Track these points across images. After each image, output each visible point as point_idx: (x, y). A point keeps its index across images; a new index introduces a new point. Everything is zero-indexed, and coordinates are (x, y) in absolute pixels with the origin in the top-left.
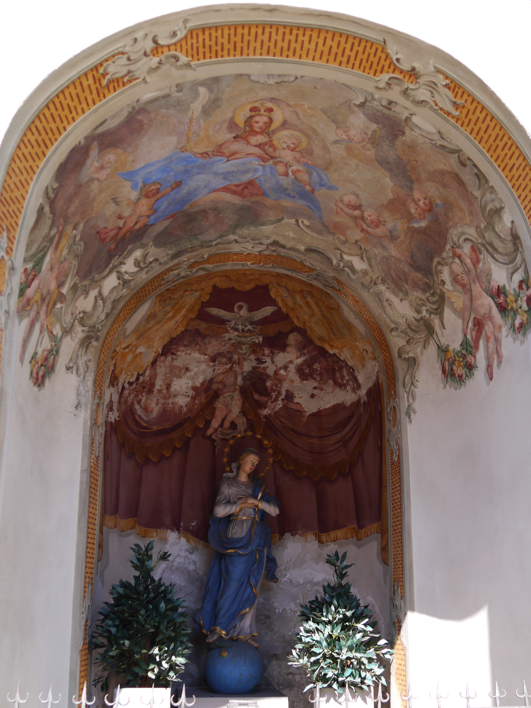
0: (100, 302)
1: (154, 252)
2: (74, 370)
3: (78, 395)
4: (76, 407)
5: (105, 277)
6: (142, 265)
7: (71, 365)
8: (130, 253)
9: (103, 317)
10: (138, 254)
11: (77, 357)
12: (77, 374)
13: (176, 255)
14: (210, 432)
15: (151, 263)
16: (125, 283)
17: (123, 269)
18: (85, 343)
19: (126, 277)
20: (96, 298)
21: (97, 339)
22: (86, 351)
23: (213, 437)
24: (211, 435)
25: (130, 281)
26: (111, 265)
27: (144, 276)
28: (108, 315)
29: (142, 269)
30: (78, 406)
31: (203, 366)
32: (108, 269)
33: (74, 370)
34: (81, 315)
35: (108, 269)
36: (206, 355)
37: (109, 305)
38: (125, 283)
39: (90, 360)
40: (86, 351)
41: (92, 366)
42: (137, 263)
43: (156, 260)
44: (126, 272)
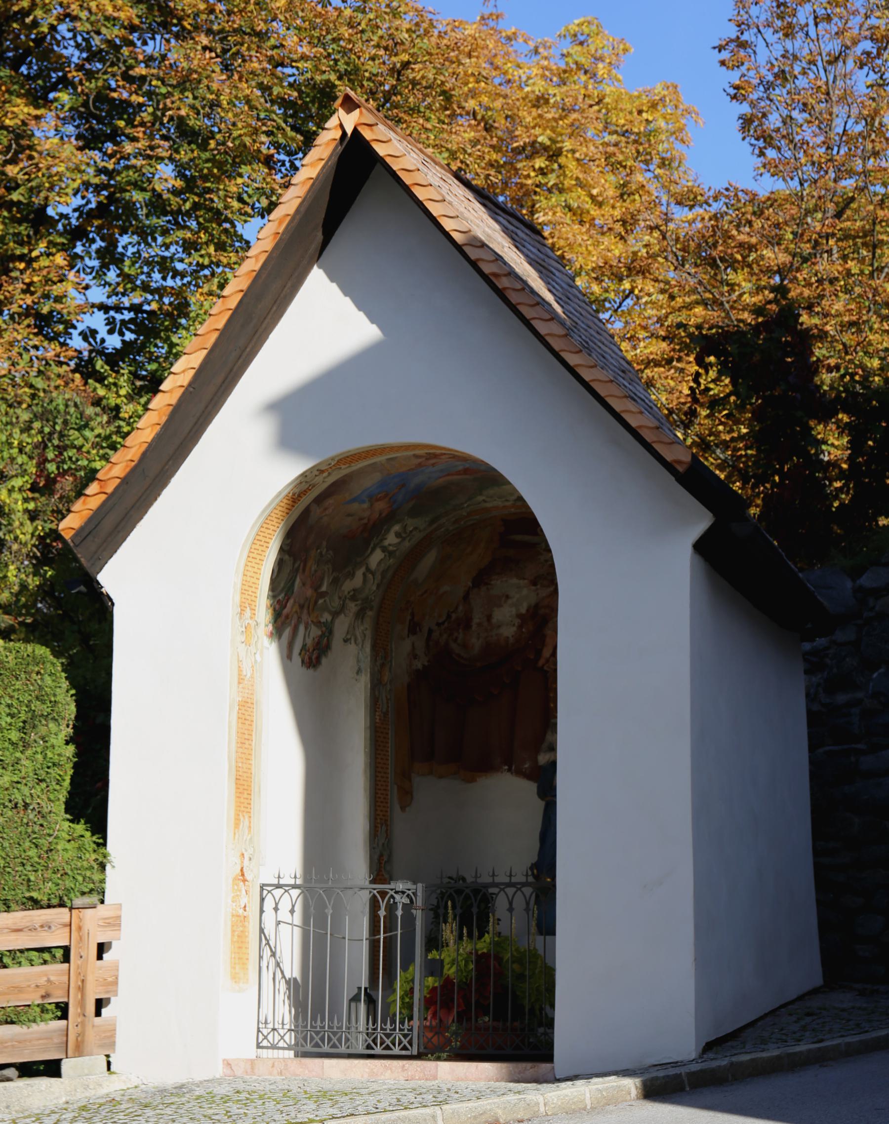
0: (370, 576)
1: (411, 523)
2: (353, 641)
3: (358, 661)
4: (357, 673)
5: (369, 556)
6: (404, 535)
7: (349, 637)
8: (388, 531)
9: (374, 588)
10: (397, 528)
11: (354, 627)
12: (356, 643)
13: (432, 522)
14: (541, 663)
15: (411, 532)
16: (391, 554)
17: (386, 543)
18: (360, 615)
19: (391, 548)
20: (364, 574)
21: (371, 609)
22: (362, 622)
23: (545, 668)
24: (543, 665)
25: (395, 551)
26: (372, 545)
27: (407, 544)
28: (378, 586)
29: (404, 539)
30: (359, 672)
31: (525, 592)
32: (370, 549)
33: (353, 641)
34: (352, 593)
35: (370, 549)
36: (524, 579)
37: (378, 577)
38: (391, 554)
39: (366, 629)
40: (362, 622)
41: (368, 633)
42: (398, 535)
43: (416, 528)
44: (390, 545)
